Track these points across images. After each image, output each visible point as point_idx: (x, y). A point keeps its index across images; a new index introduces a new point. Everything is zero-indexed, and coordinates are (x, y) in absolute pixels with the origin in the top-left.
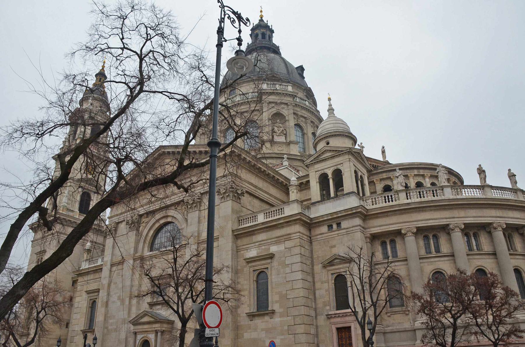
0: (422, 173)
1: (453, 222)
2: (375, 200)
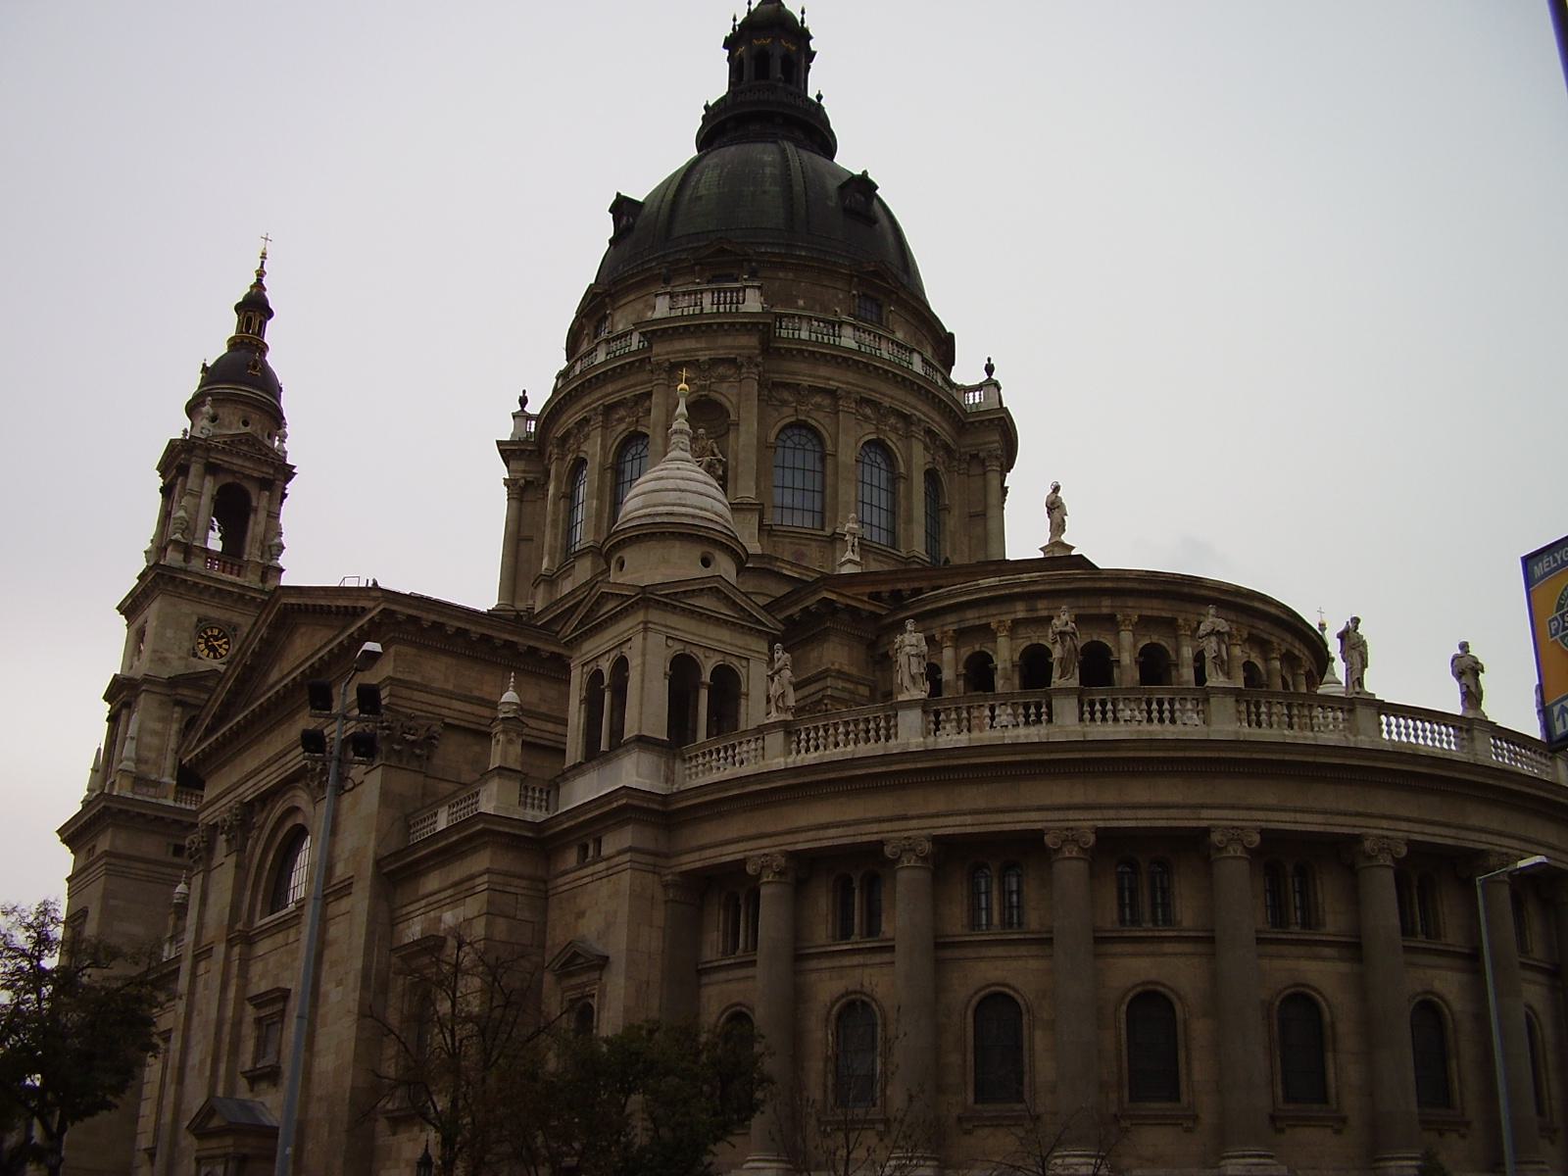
2: (808, 735)
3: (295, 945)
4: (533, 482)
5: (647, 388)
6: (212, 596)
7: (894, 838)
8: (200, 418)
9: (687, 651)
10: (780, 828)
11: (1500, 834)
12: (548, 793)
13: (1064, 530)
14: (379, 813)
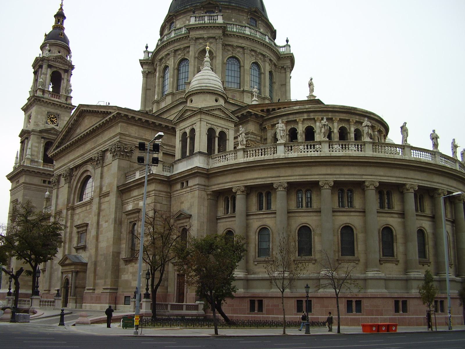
0: (312, 117)
1: (277, 181)
3: (89, 210)
4: (150, 72)
6: (51, 105)
7: (277, 182)
8: (45, 50)
9: (212, 127)
10: (243, 179)
11: (442, 184)
12: (170, 167)
13: (313, 91)
14: (117, 172)
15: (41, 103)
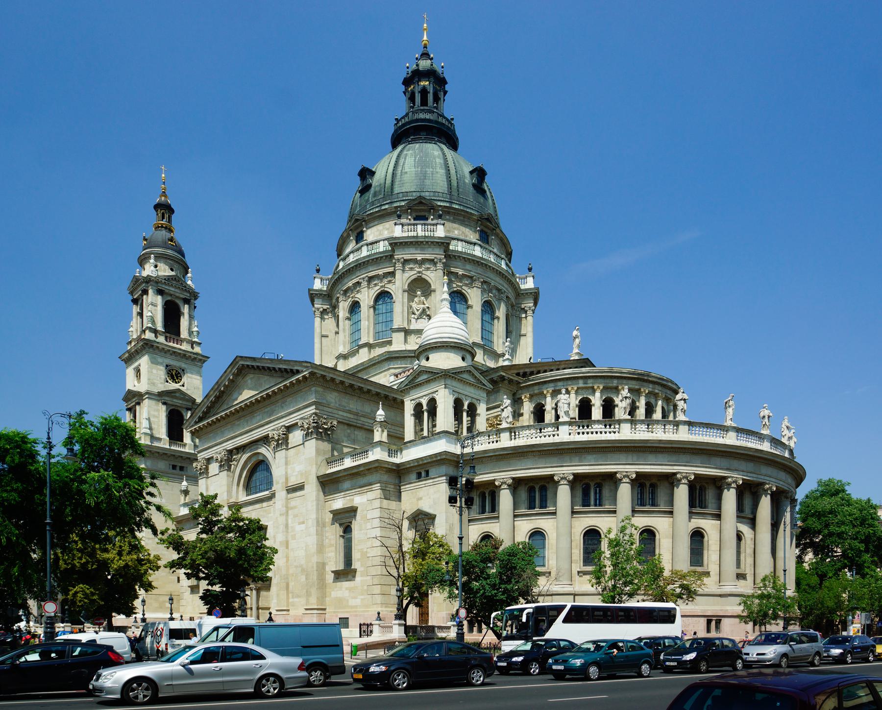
0: (591, 385)
5: (391, 269)
9: (460, 397)
15: (154, 350)
